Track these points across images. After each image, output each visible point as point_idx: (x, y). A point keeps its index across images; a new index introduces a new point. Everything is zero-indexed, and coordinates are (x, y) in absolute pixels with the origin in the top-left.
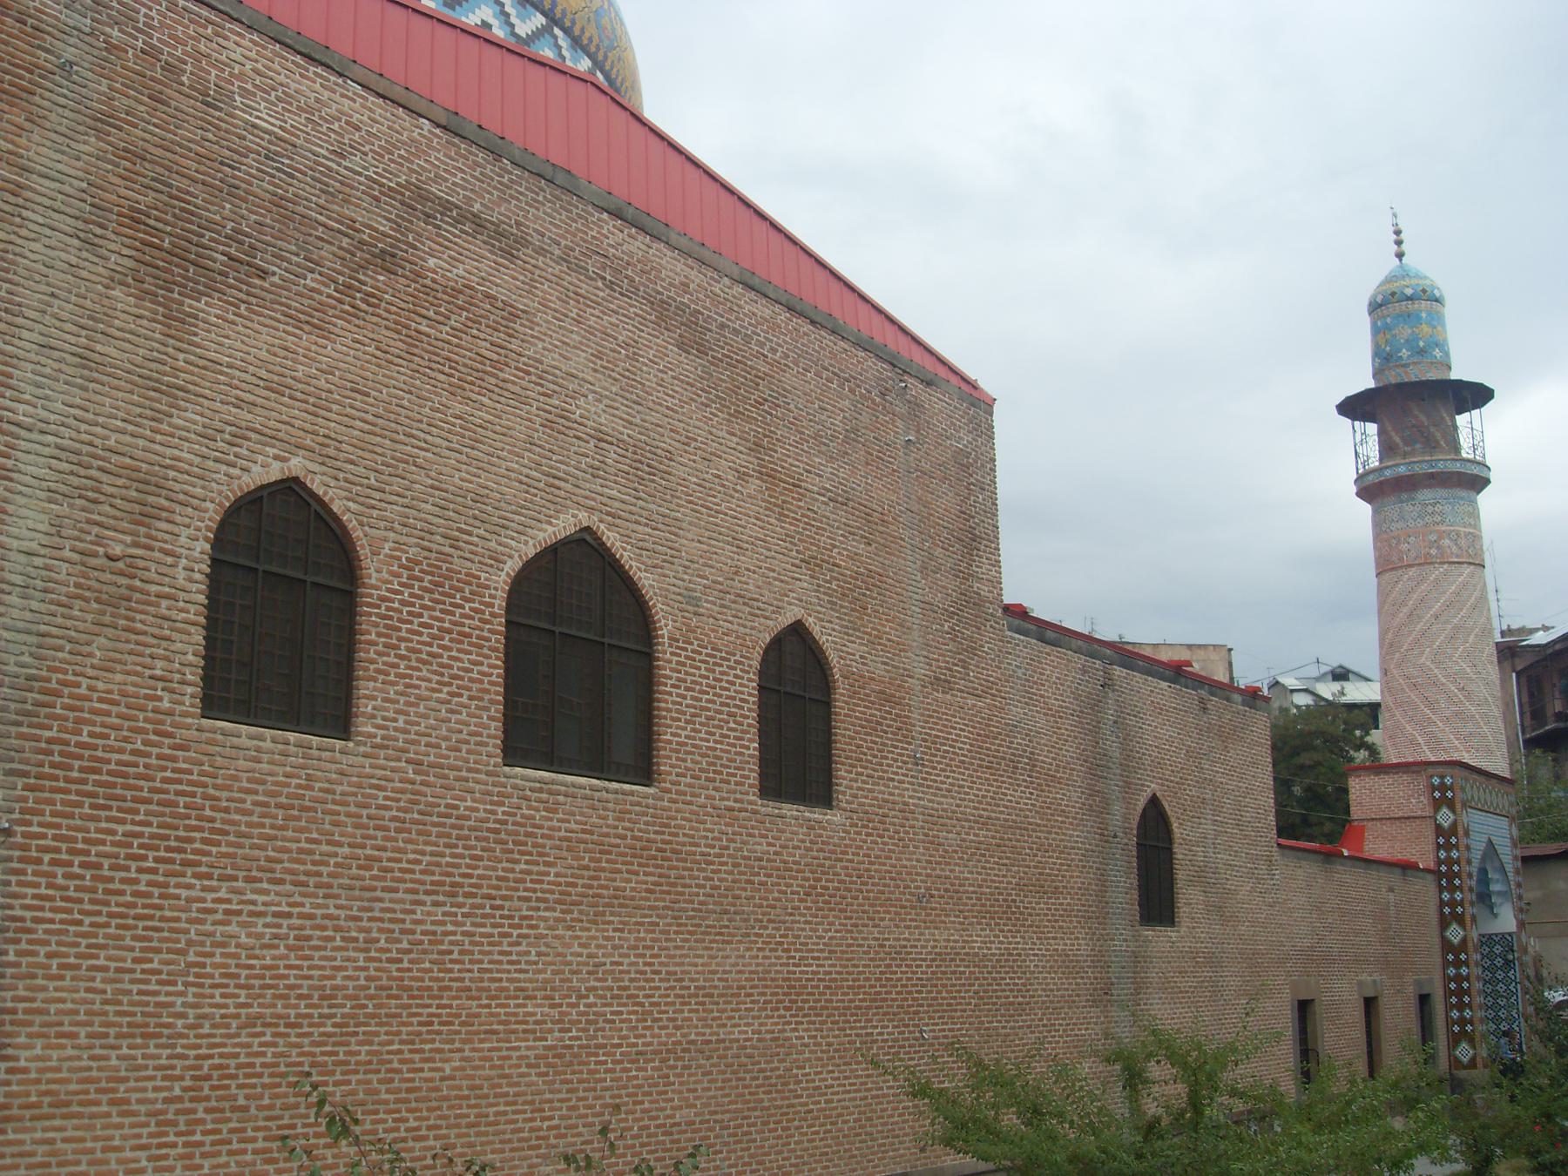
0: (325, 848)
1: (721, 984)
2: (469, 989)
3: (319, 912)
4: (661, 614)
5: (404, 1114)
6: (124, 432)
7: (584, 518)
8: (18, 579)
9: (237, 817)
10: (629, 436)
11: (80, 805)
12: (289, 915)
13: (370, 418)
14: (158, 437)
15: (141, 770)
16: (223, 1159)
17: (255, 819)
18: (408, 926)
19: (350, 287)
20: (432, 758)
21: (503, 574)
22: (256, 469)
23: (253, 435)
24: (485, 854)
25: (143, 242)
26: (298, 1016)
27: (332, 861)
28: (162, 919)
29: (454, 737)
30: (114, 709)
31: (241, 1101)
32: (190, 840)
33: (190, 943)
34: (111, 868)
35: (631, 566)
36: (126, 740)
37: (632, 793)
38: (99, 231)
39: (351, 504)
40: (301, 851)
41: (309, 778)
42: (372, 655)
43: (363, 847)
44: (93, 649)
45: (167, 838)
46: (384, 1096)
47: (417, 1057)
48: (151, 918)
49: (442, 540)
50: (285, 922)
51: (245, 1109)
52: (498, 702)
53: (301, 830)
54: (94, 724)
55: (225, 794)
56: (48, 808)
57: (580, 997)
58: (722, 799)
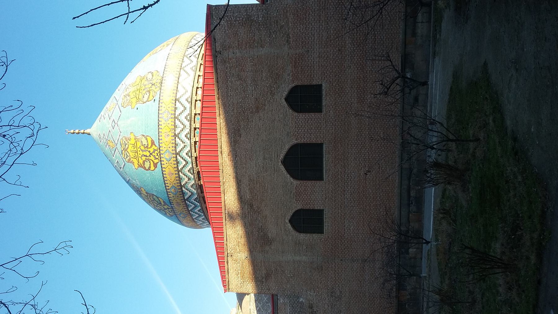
1: (358, 125)
2: (359, 187)
3: (348, 215)
4: (292, 143)
5: (377, 199)
6: (290, 247)
7: (280, 163)
8: (312, 260)
9: (336, 229)
10: (262, 151)
11: (337, 250)
12: (349, 220)
13: (276, 208)
14: (289, 242)
15: (332, 243)
17: (336, 226)
18: (350, 200)
19: (258, 212)
20: (325, 195)
21: (294, 182)
23: (285, 228)
24: (338, 184)
25: (264, 245)
26: (363, 218)
27: (341, 213)
28: (350, 239)
29: (321, 191)
30: (325, 247)
31: (374, 227)
33: (353, 235)
34: (344, 246)
35: (286, 151)
36: (328, 245)
37: (325, 150)
39: (290, 211)
40: (340, 218)
41: (330, 218)
42: (311, 207)
43: (339, 208)
44: (318, 250)
45: (340, 239)
46: (374, 203)
47: (369, 197)
48: (350, 241)
49: (291, 195)
51: (375, 226)
52: (314, 182)
53: (337, 218)
54: (327, 249)
55: (334, 230)
56: (338, 255)
57: (360, 163)
58: (324, 125)
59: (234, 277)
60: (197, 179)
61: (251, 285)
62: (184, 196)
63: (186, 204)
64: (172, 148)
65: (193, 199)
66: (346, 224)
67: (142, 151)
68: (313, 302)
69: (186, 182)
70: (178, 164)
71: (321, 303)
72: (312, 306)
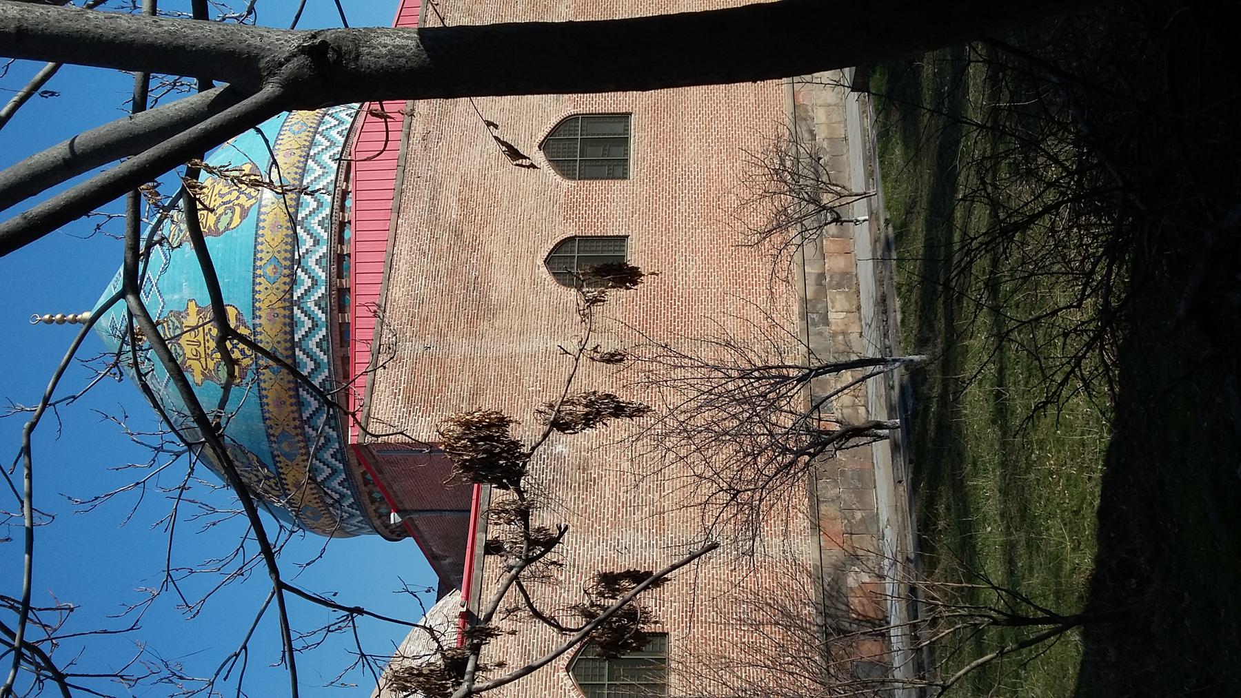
0: (664, 245)
13: (517, 237)
16: (761, 274)
22: (544, 276)
32: (665, 290)
33: (696, 288)
38: (478, 333)
50: (688, 258)
59: (385, 402)
60: (337, 241)
61: (427, 419)
62: (291, 288)
63: (292, 317)
64: (293, 175)
65: (312, 299)
66: (679, 264)
67: (222, 196)
68: (589, 454)
69: (307, 249)
70: (300, 208)
71: (612, 455)
72: (588, 465)
